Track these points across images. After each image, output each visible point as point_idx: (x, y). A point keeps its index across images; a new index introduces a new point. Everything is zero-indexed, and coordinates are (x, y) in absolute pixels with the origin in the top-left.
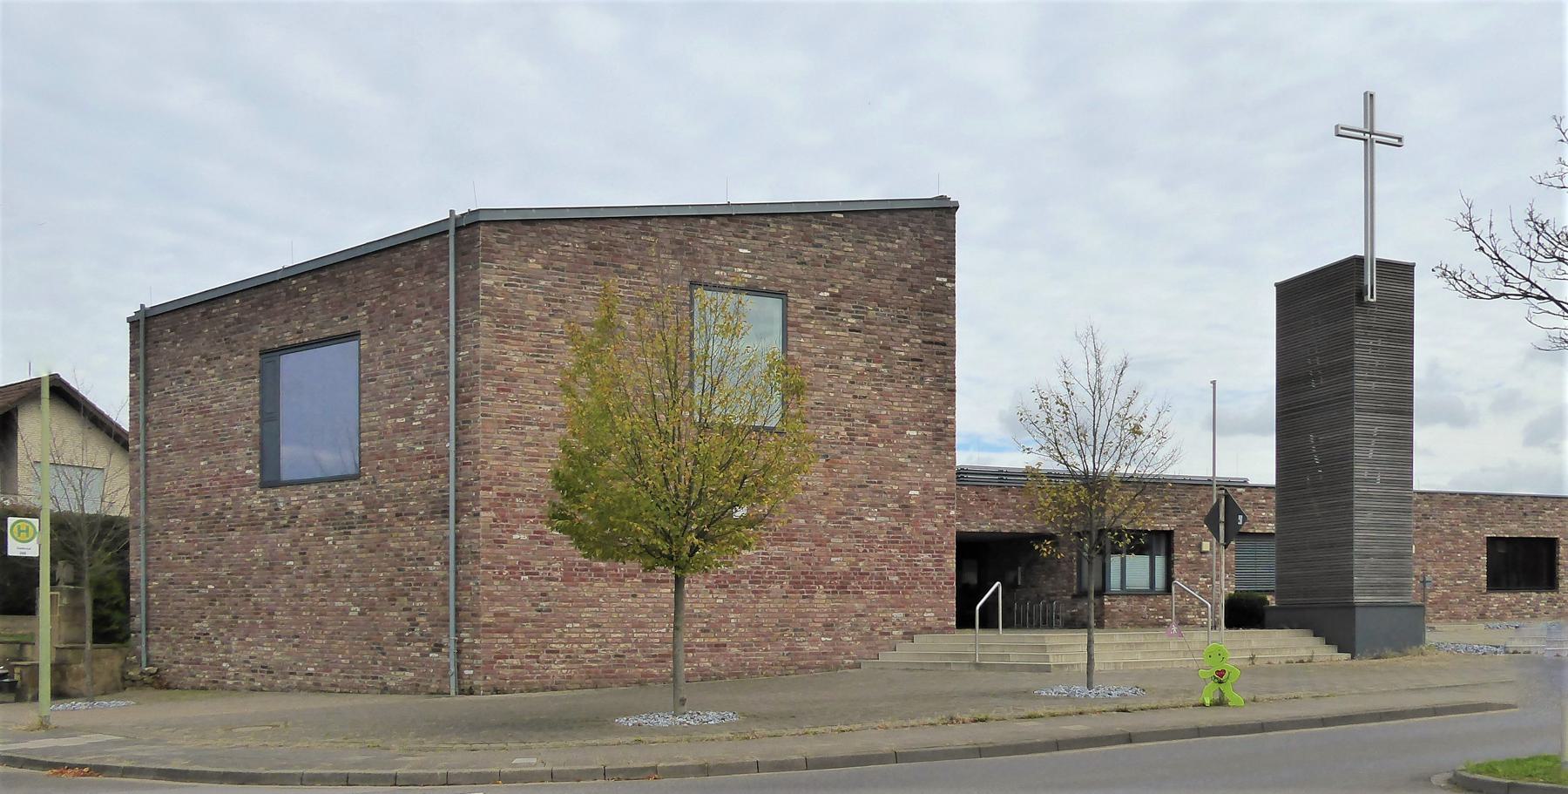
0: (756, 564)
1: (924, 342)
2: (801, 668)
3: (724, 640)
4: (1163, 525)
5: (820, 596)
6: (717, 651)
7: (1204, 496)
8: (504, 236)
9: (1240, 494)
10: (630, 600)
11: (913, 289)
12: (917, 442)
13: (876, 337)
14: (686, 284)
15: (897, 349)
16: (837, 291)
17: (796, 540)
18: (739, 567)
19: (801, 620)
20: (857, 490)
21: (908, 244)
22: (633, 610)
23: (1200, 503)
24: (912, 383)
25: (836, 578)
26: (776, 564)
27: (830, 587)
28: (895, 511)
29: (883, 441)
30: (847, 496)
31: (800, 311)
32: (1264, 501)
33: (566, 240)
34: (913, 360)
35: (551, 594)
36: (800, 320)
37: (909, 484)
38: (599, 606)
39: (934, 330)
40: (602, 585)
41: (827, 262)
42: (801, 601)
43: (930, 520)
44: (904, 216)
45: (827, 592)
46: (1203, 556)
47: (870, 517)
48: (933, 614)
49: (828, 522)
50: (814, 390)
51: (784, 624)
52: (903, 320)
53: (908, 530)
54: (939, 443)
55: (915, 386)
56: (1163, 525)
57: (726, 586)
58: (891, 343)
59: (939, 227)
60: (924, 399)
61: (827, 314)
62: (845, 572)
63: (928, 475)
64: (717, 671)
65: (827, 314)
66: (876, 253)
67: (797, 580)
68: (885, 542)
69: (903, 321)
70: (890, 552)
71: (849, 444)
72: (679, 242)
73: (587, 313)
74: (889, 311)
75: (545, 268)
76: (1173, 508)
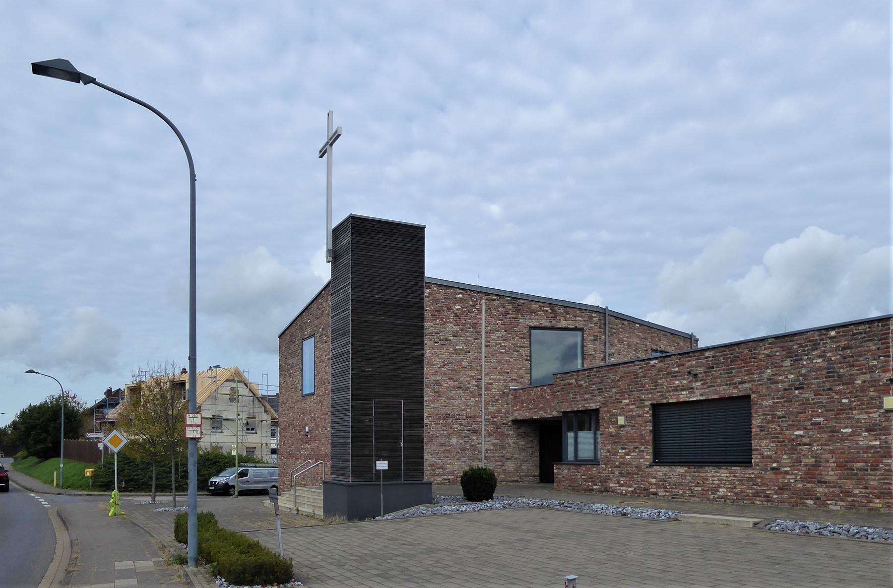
4: (591, 405)
7: (622, 374)
23: (619, 381)
32: (677, 369)
46: (622, 429)
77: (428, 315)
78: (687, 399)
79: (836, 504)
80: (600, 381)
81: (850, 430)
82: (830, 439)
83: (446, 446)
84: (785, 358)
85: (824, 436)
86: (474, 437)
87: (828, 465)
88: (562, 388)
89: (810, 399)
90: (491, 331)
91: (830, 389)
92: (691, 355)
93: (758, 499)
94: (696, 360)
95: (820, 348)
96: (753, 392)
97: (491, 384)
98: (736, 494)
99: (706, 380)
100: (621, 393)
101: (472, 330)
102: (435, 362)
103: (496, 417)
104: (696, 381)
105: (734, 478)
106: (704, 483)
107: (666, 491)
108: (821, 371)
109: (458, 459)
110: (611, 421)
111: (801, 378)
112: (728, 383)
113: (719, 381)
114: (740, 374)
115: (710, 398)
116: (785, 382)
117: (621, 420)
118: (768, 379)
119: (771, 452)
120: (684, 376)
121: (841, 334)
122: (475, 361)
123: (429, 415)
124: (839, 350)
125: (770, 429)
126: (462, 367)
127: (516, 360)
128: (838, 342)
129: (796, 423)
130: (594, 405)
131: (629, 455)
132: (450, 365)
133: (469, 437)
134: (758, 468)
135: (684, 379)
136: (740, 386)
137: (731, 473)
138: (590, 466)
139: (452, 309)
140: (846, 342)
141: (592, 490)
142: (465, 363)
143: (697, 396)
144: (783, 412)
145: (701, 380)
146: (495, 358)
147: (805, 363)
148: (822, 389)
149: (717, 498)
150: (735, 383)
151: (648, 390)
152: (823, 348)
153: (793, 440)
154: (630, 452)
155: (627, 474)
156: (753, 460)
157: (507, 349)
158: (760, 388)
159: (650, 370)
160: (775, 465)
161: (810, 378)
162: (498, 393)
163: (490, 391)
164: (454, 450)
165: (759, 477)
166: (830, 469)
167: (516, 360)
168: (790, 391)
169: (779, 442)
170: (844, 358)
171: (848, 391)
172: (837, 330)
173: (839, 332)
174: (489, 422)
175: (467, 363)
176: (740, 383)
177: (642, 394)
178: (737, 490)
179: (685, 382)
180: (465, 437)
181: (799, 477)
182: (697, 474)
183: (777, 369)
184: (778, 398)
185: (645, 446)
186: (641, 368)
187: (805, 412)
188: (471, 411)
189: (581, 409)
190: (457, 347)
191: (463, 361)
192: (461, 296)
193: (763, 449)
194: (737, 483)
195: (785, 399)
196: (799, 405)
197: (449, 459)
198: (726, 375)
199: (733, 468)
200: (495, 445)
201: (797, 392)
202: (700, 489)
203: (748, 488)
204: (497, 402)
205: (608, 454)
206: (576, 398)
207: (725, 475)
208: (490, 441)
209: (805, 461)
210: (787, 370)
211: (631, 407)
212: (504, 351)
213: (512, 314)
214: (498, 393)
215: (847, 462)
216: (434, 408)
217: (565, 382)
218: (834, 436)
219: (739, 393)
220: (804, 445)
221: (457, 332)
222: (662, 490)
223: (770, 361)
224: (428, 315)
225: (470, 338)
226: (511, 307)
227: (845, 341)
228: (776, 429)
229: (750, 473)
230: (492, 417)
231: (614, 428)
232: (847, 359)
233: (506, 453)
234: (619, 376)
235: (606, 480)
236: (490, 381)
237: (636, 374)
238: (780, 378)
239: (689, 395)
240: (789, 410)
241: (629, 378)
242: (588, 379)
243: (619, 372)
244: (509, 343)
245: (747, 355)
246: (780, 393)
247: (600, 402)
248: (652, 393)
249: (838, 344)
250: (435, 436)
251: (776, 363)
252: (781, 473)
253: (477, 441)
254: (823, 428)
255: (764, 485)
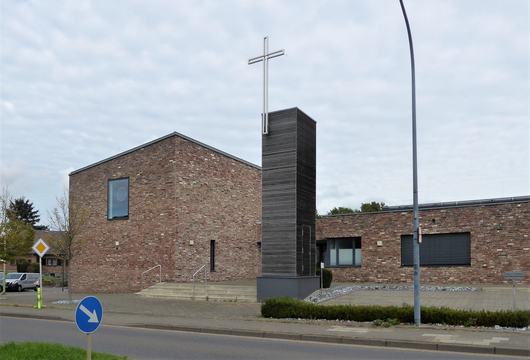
0: (121, 259)
1: (166, 183)
2: (132, 291)
3: (114, 281)
4: (355, 234)
5: (137, 269)
6: (112, 285)
7: (380, 218)
8: (73, 178)
9: (404, 215)
10: (94, 270)
11: (163, 166)
12: (163, 217)
13: (152, 185)
14: (107, 180)
15: (157, 187)
16: (142, 173)
17: (131, 252)
18: (117, 260)
19: (132, 276)
20: (147, 235)
21: (161, 152)
22: (95, 272)
23: (377, 222)
24: (162, 198)
25: (141, 263)
26: (126, 259)
27: (139, 266)
28: (157, 241)
29: (154, 218)
30: (144, 237)
31: (133, 181)
33: (84, 176)
34: (162, 190)
35: (80, 268)
36: (132, 184)
37: (161, 231)
38: (89, 271)
39: (169, 178)
40: (89, 265)
41: (139, 164)
42: (132, 270)
43: (167, 243)
44: (160, 143)
45: (139, 268)
46: (379, 248)
47: (150, 243)
48: (168, 275)
49: (139, 246)
50: (136, 205)
51: (128, 277)
52: (159, 177)
53: (161, 247)
54: (170, 217)
55: (163, 199)
56: (355, 234)
57: (114, 266)
58: (156, 186)
59: (170, 143)
60: (166, 202)
61: (139, 180)
62: (143, 261)
63: (166, 228)
64: (112, 290)
65: (139, 180)
66: (152, 158)
67: (131, 264)
68: (154, 251)
69: (159, 177)
70: (155, 254)
71: (145, 220)
72: (105, 169)
73: (87, 194)
74: (156, 175)
75: (80, 184)
76: (360, 226)
77: (219, 174)
78: (428, 233)
79: (520, 282)
80: (362, 222)
81: (528, 249)
82: (517, 253)
83: (227, 257)
84: (491, 215)
85: (514, 251)
86: (240, 252)
87: (516, 264)
88: (330, 225)
89: (506, 235)
90: (248, 187)
91: (517, 230)
92: (430, 211)
93: (475, 281)
94: (434, 213)
95: (512, 211)
96: (472, 231)
97: (248, 220)
98: (461, 280)
99: (441, 224)
100: (379, 228)
101: (239, 186)
102: (222, 204)
103: (250, 240)
104: (434, 224)
105: (459, 272)
106: (439, 275)
107: (412, 280)
108: (513, 222)
109: (233, 265)
110: (371, 244)
111: (501, 225)
112: (456, 226)
113: (449, 225)
114: (464, 222)
115: (444, 233)
116: (491, 226)
117: (380, 243)
118: (481, 225)
119: (483, 259)
120: (426, 221)
121: (524, 206)
122: (241, 205)
123: (219, 237)
124: (523, 213)
125: (482, 248)
126: (235, 209)
127: (259, 206)
128: (522, 209)
129: (498, 246)
130: (357, 234)
131: (384, 262)
132: (229, 206)
133: (238, 252)
134: (474, 267)
135: (426, 223)
136: (463, 228)
137: (457, 269)
138: (353, 268)
139: (230, 172)
140: (527, 210)
141: (356, 281)
142: (236, 206)
143: (435, 231)
144: (490, 240)
145: (437, 224)
146: (250, 204)
147: (503, 218)
148: (513, 230)
149: (448, 282)
150: (461, 226)
151: (399, 227)
152: (514, 212)
153: (496, 253)
154: (386, 260)
155: (383, 271)
156: (471, 263)
157: (255, 199)
158: (477, 228)
159: (401, 217)
160: (485, 265)
161: (506, 225)
162: (251, 225)
163: (248, 224)
164: (231, 259)
165: (475, 271)
166: (517, 267)
167: (259, 206)
168: (495, 231)
169: (487, 254)
170: (525, 217)
171: (528, 231)
172: (521, 204)
173: (523, 205)
174: (247, 243)
175: (237, 206)
176: (463, 226)
177: (395, 229)
178: (461, 278)
179: (426, 224)
180: (236, 252)
181: (499, 270)
182: (435, 270)
183: (487, 220)
184: (487, 234)
185: (397, 257)
186: (394, 216)
187: (503, 241)
188: (239, 236)
189: (346, 237)
190: (232, 196)
191: (235, 205)
192: (234, 164)
193: (478, 258)
194: (461, 274)
195: (491, 234)
196: (500, 237)
197: (228, 265)
198: (455, 222)
199: (459, 267)
200: (250, 257)
201: (498, 231)
202: (437, 278)
203: (469, 277)
204: (251, 231)
205: (368, 261)
206: (342, 230)
207: (454, 271)
208: (247, 255)
209: (503, 263)
210: (493, 221)
211: (386, 236)
212: (254, 200)
213: (257, 179)
214: (251, 225)
215: (526, 263)
216: (221, 233)
217: (333, 221)
218: (520, 252)
219: (462, 231)
220: (502, 256)
221: (233, 186)
222: (409, 279)
223: (482, 216)
224: (219, 174)
225: (239, 191)
226: (257, 174)
227: (526, 209)
228: (486, 248)
229: (469, 269)
230: (248, 240)
231: (373, 247)
232: (527, 218)
233: (254, 262)
234: (377, 220)
235: (368, 275)
236: (248, 218)
237: (390, 219)
238: (489, 224)
239: (429, 231)
240: (494, 239)
241: (385, 221)
242: (352, 220)
243: (377, 217)
244: (256, 196)
245: (468, 213)
246: (488, 231)
247: (362, 233)
248: (402, 229)
249: (522, 210)
250: (222, 250)
251: (486, 217)
252: (489, 269)
253: (242, 254)
254: (513, 248)
255: (479, 275)
